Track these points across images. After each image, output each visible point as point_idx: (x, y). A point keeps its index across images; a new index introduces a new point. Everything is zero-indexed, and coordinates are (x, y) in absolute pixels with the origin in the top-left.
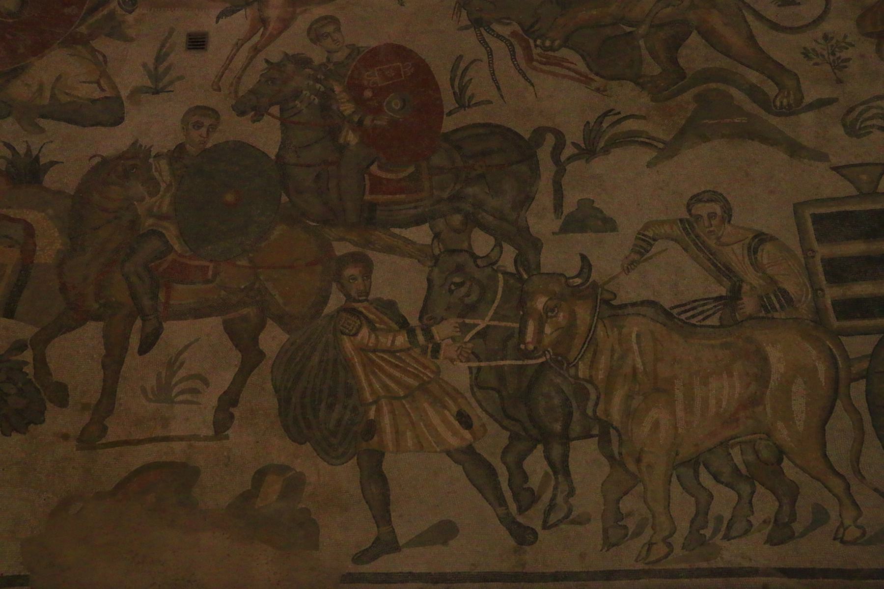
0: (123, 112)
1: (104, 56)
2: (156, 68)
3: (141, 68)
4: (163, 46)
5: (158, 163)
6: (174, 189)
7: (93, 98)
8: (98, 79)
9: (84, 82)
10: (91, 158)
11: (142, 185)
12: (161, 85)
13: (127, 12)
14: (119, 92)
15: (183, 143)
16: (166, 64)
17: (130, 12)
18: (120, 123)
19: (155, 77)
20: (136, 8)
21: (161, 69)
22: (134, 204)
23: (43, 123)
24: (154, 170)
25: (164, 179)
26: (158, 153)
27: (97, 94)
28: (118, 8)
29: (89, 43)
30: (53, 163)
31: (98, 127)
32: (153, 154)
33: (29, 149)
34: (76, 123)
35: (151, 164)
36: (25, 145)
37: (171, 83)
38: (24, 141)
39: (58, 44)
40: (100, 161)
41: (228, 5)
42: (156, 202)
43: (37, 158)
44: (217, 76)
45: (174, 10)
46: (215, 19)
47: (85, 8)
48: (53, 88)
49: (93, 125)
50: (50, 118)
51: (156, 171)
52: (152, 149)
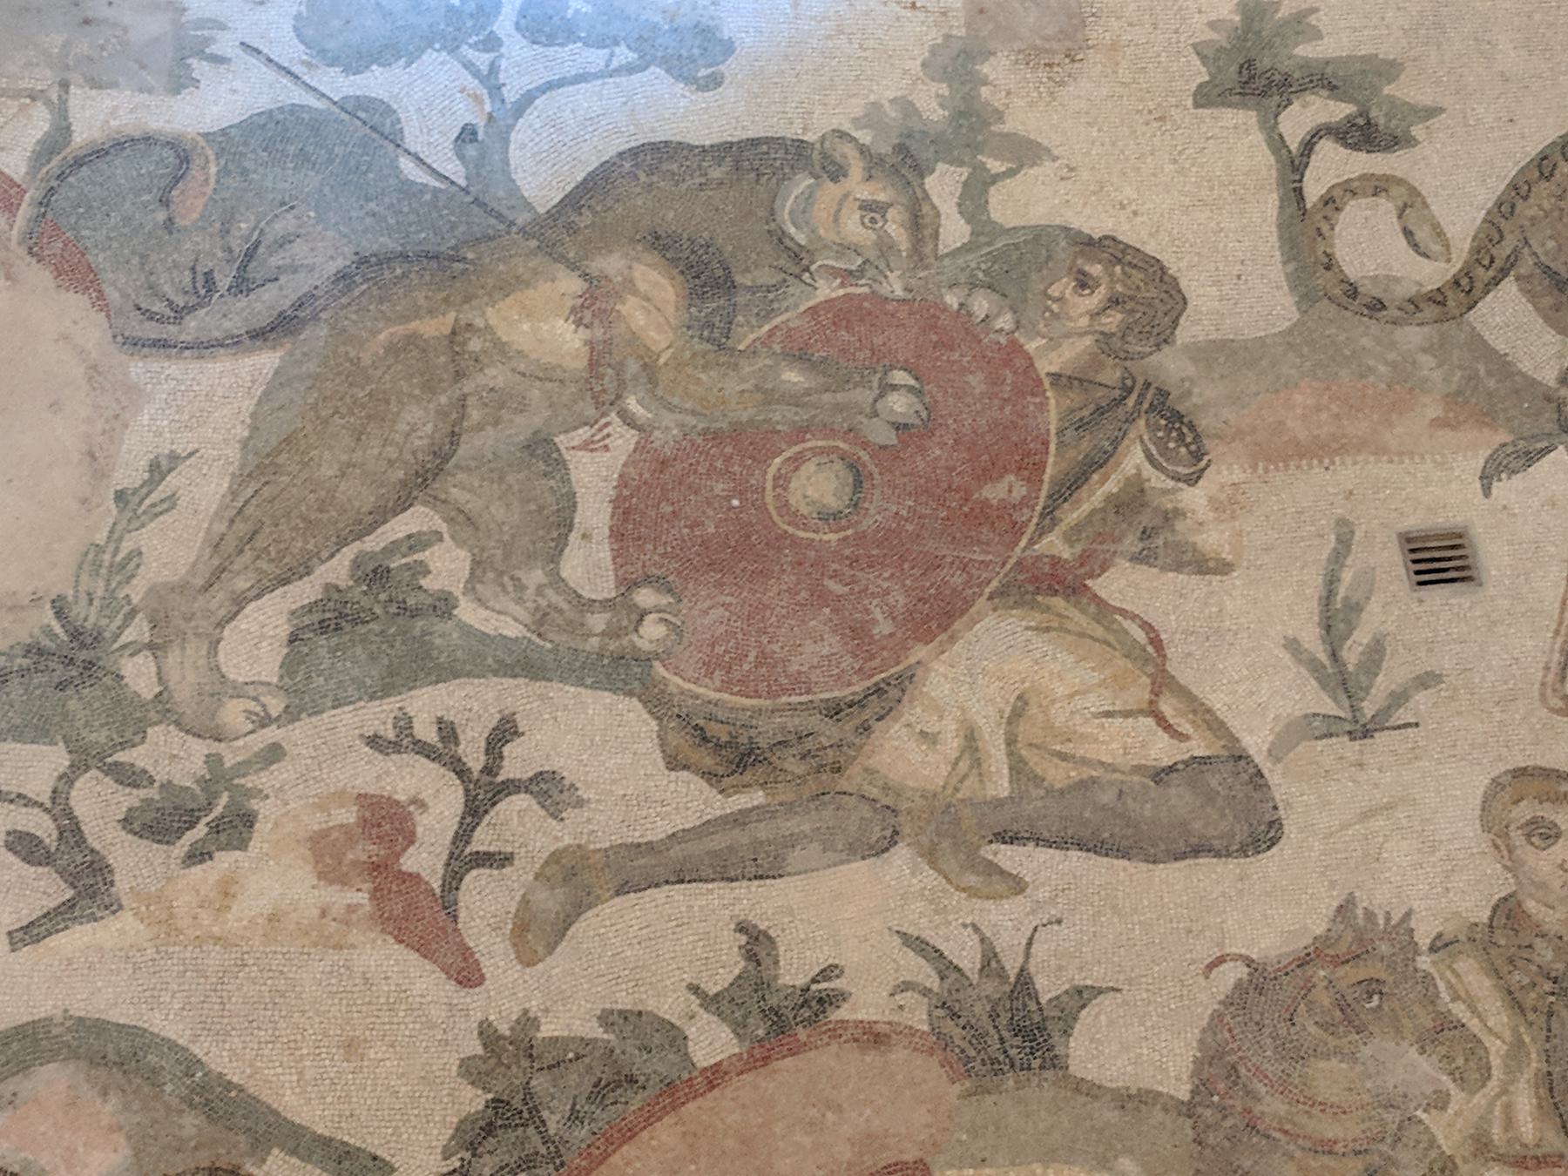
0: (1271, 804)
1: (1147, 626)
2: (1334, 655)
3: (1286, 657)
4: (1332, 581)
5: (1453, 971)
6: (1534, 1056)
7: (1154, 763)
8: (1151, 702)
9: (1108, 714)
10: (1212, 966)
11: (1422, 1051)
12: (1369, 708)
13: (1179, 480)
14: (1237, 740)
15: (1511, 896)
16: (1361, 637)
17: (1193, 480)
18: (1273, 842)
19: (1343, 683)
20: (1208, 465)
21: (1352, 655)
22: (1420, 1121)
23: (1008, 857)
24: (1445, 996)
25: (1489, 1024)
26: (1439, 936)
27: (1162, 751)
28: (1148, 471)
29: (1085, 586)
30: (1082, 995)
31: (1201, 861)
32: (1424, 942)
33: (990, 959)
34: (1126, 855)
35: (1427, 975)
36: (973, 942)
37: (1399, 698)
38: (965, 926)
39: (990, 598)
40: (1245, 977)
41: (1503, 437)
42: (1491, 1104)
43: (1024, 981)
44: (1547, 668)
45: (1333, 463)
46: (1478, 485)
47: (1046, 477)
48: (1011, 741)
49: (1182, 856)
50: (1028, 839)
51: (1453, 1000)
52: (1413, 924)
